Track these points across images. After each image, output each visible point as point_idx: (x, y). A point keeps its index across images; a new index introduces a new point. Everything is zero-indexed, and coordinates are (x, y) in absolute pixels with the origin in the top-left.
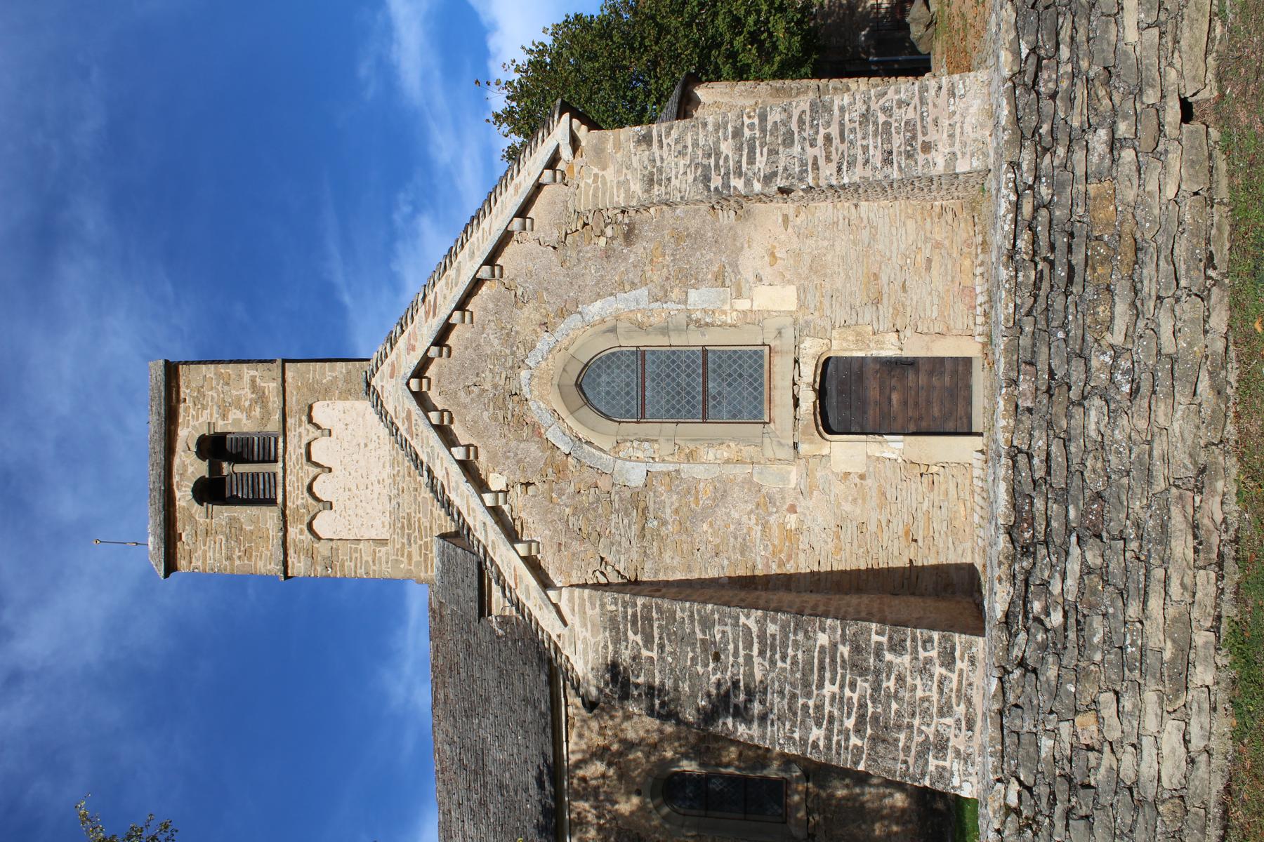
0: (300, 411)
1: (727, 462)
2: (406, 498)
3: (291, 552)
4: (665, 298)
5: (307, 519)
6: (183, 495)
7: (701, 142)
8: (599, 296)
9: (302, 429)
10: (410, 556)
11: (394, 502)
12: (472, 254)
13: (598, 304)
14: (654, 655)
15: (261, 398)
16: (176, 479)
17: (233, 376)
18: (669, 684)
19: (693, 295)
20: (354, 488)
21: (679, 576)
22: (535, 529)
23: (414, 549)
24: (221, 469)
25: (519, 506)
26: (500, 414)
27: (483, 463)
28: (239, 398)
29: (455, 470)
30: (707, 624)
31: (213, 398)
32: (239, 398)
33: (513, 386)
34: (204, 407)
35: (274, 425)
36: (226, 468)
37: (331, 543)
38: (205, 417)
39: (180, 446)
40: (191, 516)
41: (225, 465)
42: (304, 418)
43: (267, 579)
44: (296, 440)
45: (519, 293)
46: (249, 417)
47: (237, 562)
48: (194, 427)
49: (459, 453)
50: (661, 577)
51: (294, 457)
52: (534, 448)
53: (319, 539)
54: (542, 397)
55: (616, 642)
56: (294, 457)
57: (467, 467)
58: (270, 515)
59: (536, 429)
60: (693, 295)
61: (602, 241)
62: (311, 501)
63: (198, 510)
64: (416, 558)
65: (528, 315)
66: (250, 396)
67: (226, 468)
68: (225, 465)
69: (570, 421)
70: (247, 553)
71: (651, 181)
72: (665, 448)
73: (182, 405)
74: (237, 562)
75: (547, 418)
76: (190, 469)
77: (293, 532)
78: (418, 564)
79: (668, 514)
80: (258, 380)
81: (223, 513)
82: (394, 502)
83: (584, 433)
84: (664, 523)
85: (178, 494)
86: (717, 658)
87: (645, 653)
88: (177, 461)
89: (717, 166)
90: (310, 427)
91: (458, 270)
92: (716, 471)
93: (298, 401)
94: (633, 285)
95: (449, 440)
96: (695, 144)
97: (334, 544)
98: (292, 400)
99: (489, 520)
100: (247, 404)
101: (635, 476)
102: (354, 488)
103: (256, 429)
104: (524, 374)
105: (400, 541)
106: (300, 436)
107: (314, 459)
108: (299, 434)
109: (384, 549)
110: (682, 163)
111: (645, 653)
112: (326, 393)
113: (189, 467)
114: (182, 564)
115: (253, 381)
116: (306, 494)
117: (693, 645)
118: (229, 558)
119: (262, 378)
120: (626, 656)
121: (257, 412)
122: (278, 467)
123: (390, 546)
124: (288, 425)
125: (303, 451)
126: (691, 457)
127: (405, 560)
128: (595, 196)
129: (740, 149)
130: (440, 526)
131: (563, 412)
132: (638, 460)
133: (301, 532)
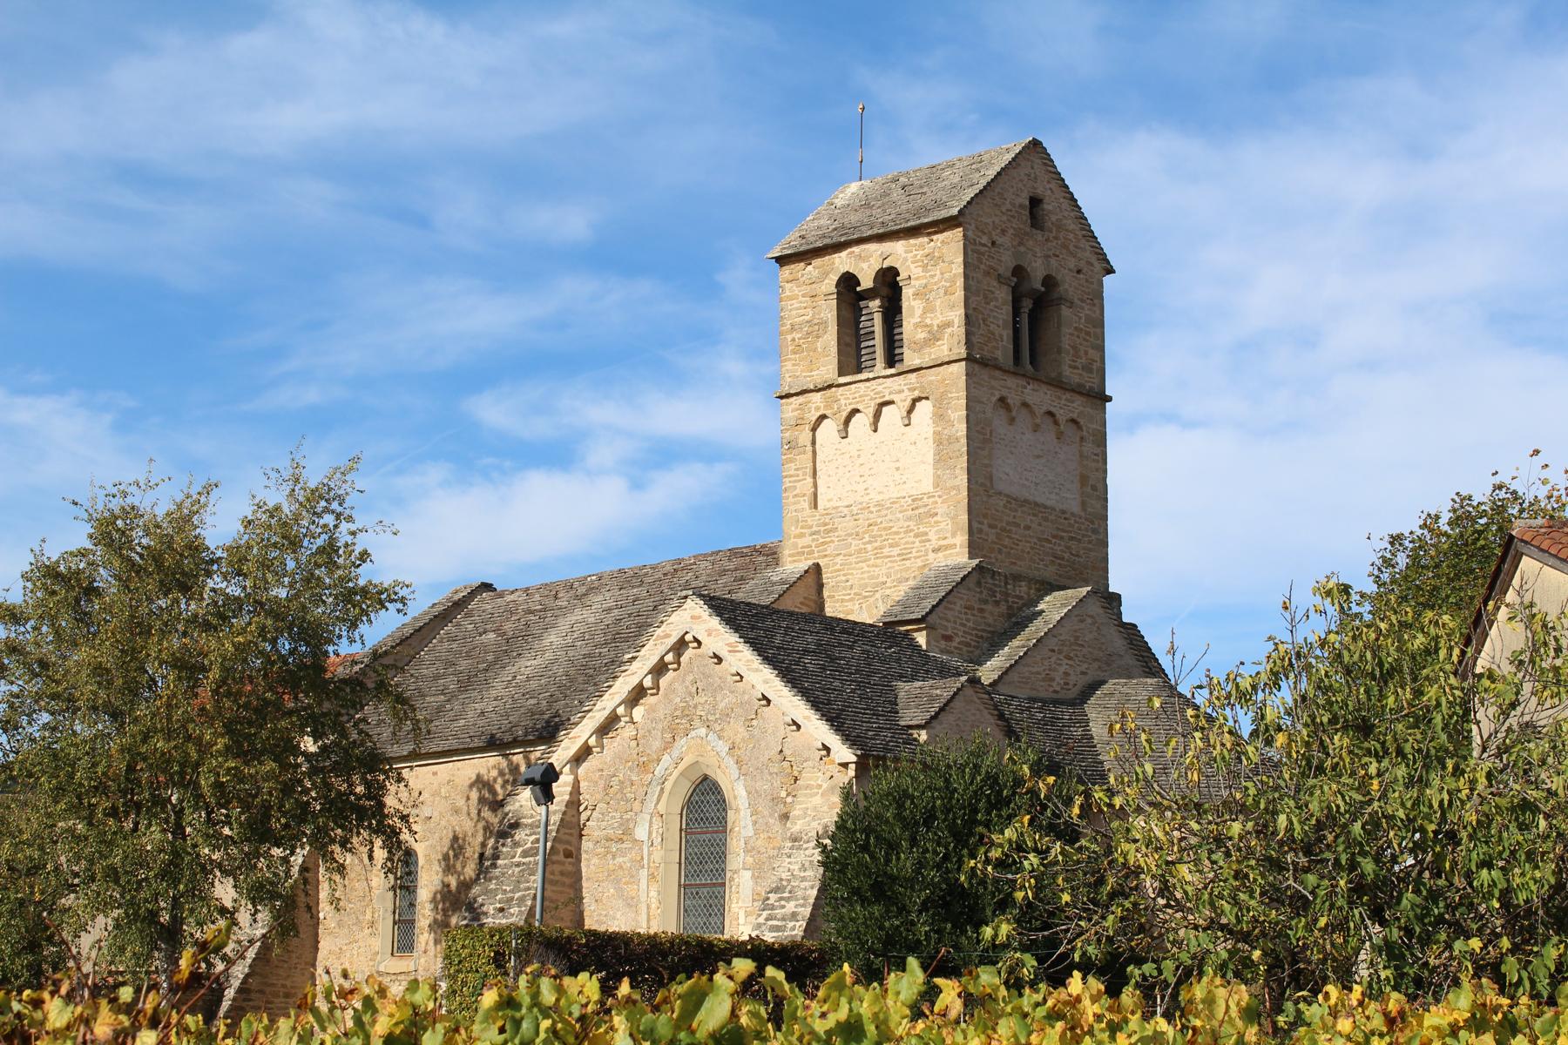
0: (922, 388)
1: (648, 907)
2: (846, 525)
3: (801, 399)
4: (746, 851)
5: (828, 413)
6: (842, 262)
7: (803, 885)
8: (749, 793)
9: (907, 393)
10: (802, 535)
11: (846, 511)
12: (766, 682)
13: (744, 793)
14: (517, 859)
15: (934, 338)
16: (856, 249)
17: (952, 298)
18: (497, 872)
19: (748, 874)
20: (861, 461)
21: (584, 870)
22: (613, 745)
23: (807, 540)
24: (873, 298)
25: (625, 732)
26: (678, 713)
27: (649, 700)
28: (932, 310)
29: (634, 681)
30: (522, 900)
31: (932, 276)
32: (932, 310)
33: (697, 722)
34: (925, 267)
35: (911, 358)
36: (875, 304)
37: (809, 444)
38: (916, 271)
39: (887, 247)
40: (826, 274)
41: (877, 302)
42: (916, 394)
43: (969, 247)
44: (897, 388)
45: (754, 723)
46: (916, 326)
47: (789, 337)
48: (906, 259)
49: (648, 682)
50: (584, 856)
51: (880, 388)
52: (657, 744)
53: (814, 430)
54: (689, 748)
55: (532, 826)
56: (880, 388)
57: (638, 694)
58: (827, 368)
59: (667, 746)
60: (748, 874)
61: (783, 794)
62: (845, 414)
63: (830, 284)
64: (801, 542)
65: (737, 730)
66: (936, 322)
67: (875, 304)
68: (877, 302)
69: (676, 773)
70: (798, 349)
71: (795, 840)
72: (658, 855)
73: (926, 239)
74: (789, 337)
75: (676, 753)
76: (865, 266)
77: (817, 397)
78: (795, 545)
79: (619, 860)
80: (949, 330)
81: (829, 311)
82: (846, 511)
83: (668, 785)
84: (614, 857)
85: (844, 254)
86: (502, 910)
87: (520, 850)
88: (872, 247)
89: (781, 899)
90: (908, 403)
91: (757, 670)
92: (643, 899)
93: (931, 382)
94: (755, 823)
95: (660, 669)
96: (803, 879)
97: (809, 448)
98: (931, 376)
99: (606, 713)
100: (928, 321)
101: (641, 833)
102: (861, 461)
103: (905, 336)
104: (703, 731)
105: (814, 519)
106: (901, 391)
107: (885, 409)
108: (899, 388)
109: (806, 505)
110: (796, 867)
111: (520, 850)
112: (940, 416)
113: (865, 263)
114: (787, 272)
115: (949, 324)
116: (849, 408)
117: (512, 891)
118: (793, 328)
119: (952, 335)
120: (520, 835)
121: (921, 335)
122: (880, 368)
123: (808, 511)
124: (910, 376)
125: (887, 398)
126: (652, 876)
127: (799, 531)
128: (807, 787)
129: (783, 919)
130: (828, 566)
131: (682, 766)
132: (650, 833)
133: (818, 409)
